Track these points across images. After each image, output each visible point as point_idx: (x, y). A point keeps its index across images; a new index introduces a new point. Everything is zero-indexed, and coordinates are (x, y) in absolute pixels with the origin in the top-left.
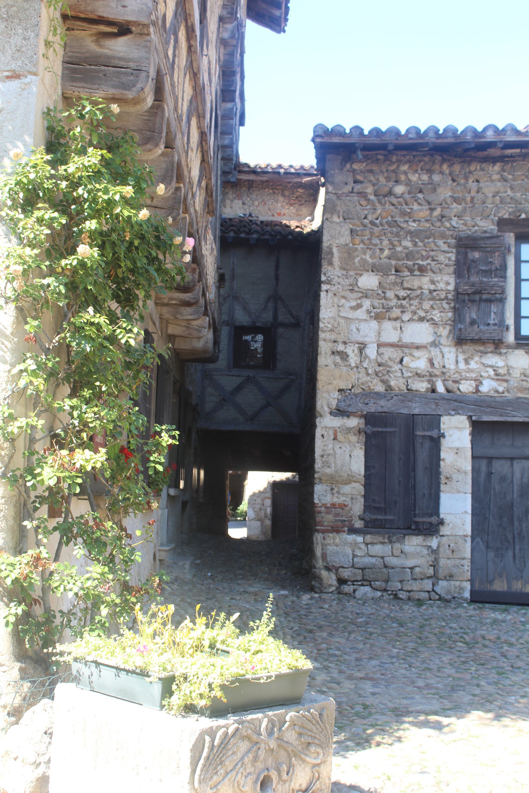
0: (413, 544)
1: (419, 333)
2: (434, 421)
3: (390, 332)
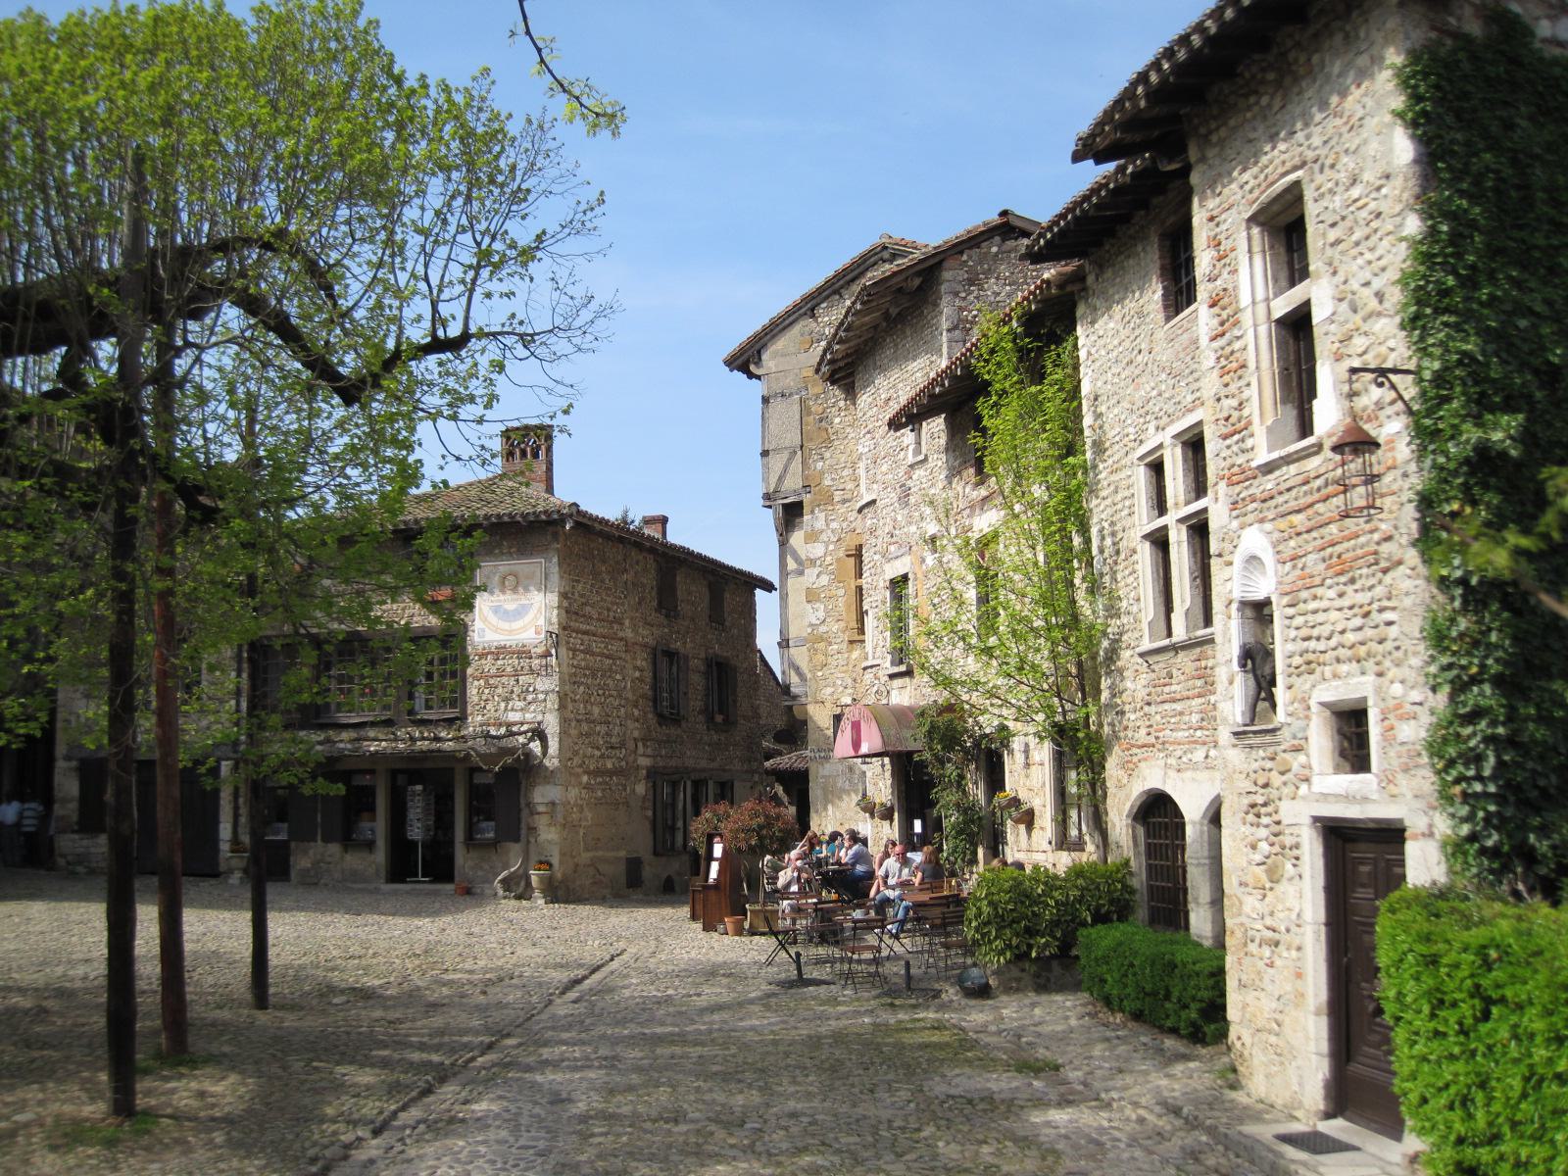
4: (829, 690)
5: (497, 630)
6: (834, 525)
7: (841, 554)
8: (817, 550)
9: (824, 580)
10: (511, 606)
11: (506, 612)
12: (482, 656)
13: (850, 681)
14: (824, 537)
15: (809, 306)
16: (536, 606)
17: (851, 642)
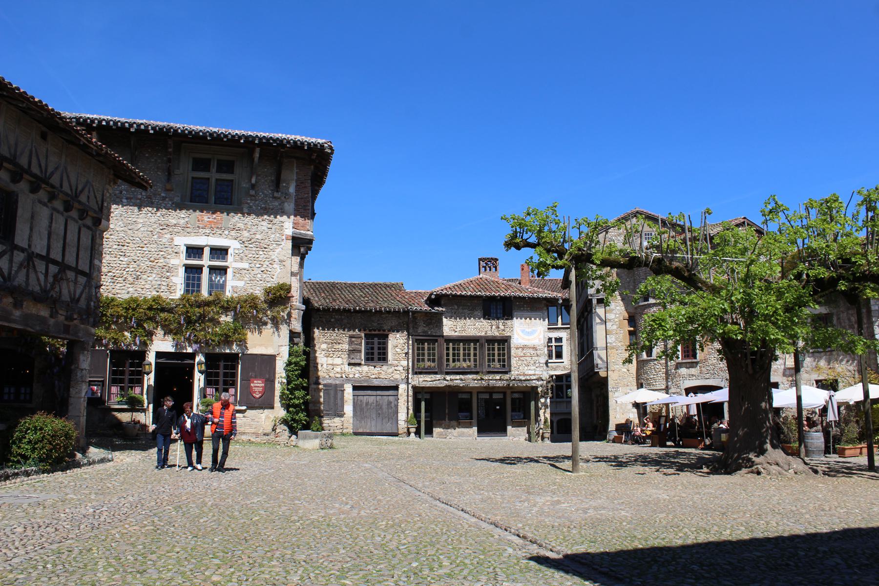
0: (337, 419)
1: (338, 361)
2: (342, 386)
3: (330, 361)
5: (523, 339)
9: (615, 327)
12: (517, 348)
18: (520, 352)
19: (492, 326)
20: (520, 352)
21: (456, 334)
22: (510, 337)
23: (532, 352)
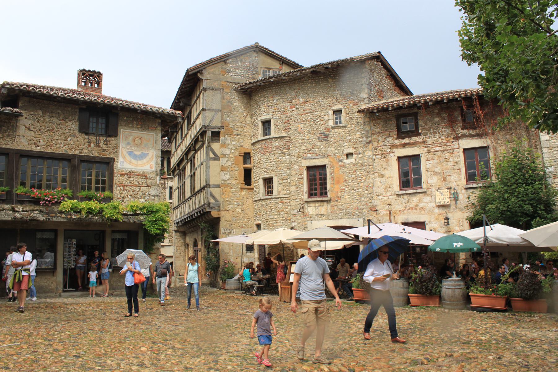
4: (231, 206)
5: (130, 163)
6: (233, 143)
7: (237, 154)
8: (227, 151)
9: (230, 163)
10: (138, 153)
11: (135, 155)
12: (122, 175)
13: (241, 203)
14: (230, 147)
15: (284, 61)
16: (150, 155)
17: (241, 188)
18: (125, 180)
19: (90, 143)
20: (125, 180)
21: (38, 149)
22: (113, 160)
23: (141, 181)
